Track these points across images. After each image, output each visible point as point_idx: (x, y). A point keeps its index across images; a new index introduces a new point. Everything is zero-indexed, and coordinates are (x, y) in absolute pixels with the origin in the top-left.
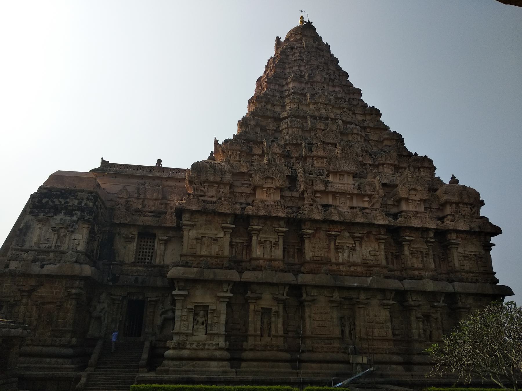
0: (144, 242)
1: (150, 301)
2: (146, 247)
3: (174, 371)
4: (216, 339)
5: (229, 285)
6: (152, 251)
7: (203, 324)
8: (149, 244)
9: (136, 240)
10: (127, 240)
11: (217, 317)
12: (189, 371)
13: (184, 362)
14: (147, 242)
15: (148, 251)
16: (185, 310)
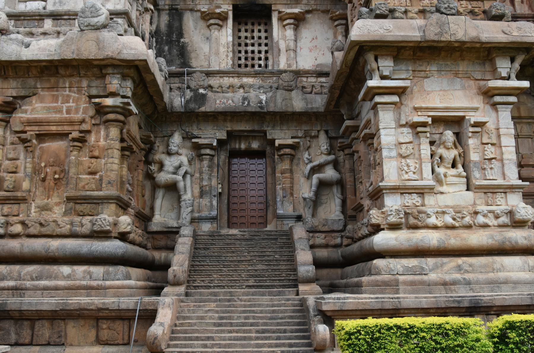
0: (246, 31)
1: (282, 147)
2: (252, 41)
3: (412, 283)
4: (499, 198)
5: (512, 60)
6: (266, 48)
7: (454, 166)
8: (256, 34)
9: (230, 21)
10: (212, 21)
11: (493, 144)
12: (454, 283)
13: (431, 261)
14: (253, 31)
15: (256, 48)
16: (406, 130)
